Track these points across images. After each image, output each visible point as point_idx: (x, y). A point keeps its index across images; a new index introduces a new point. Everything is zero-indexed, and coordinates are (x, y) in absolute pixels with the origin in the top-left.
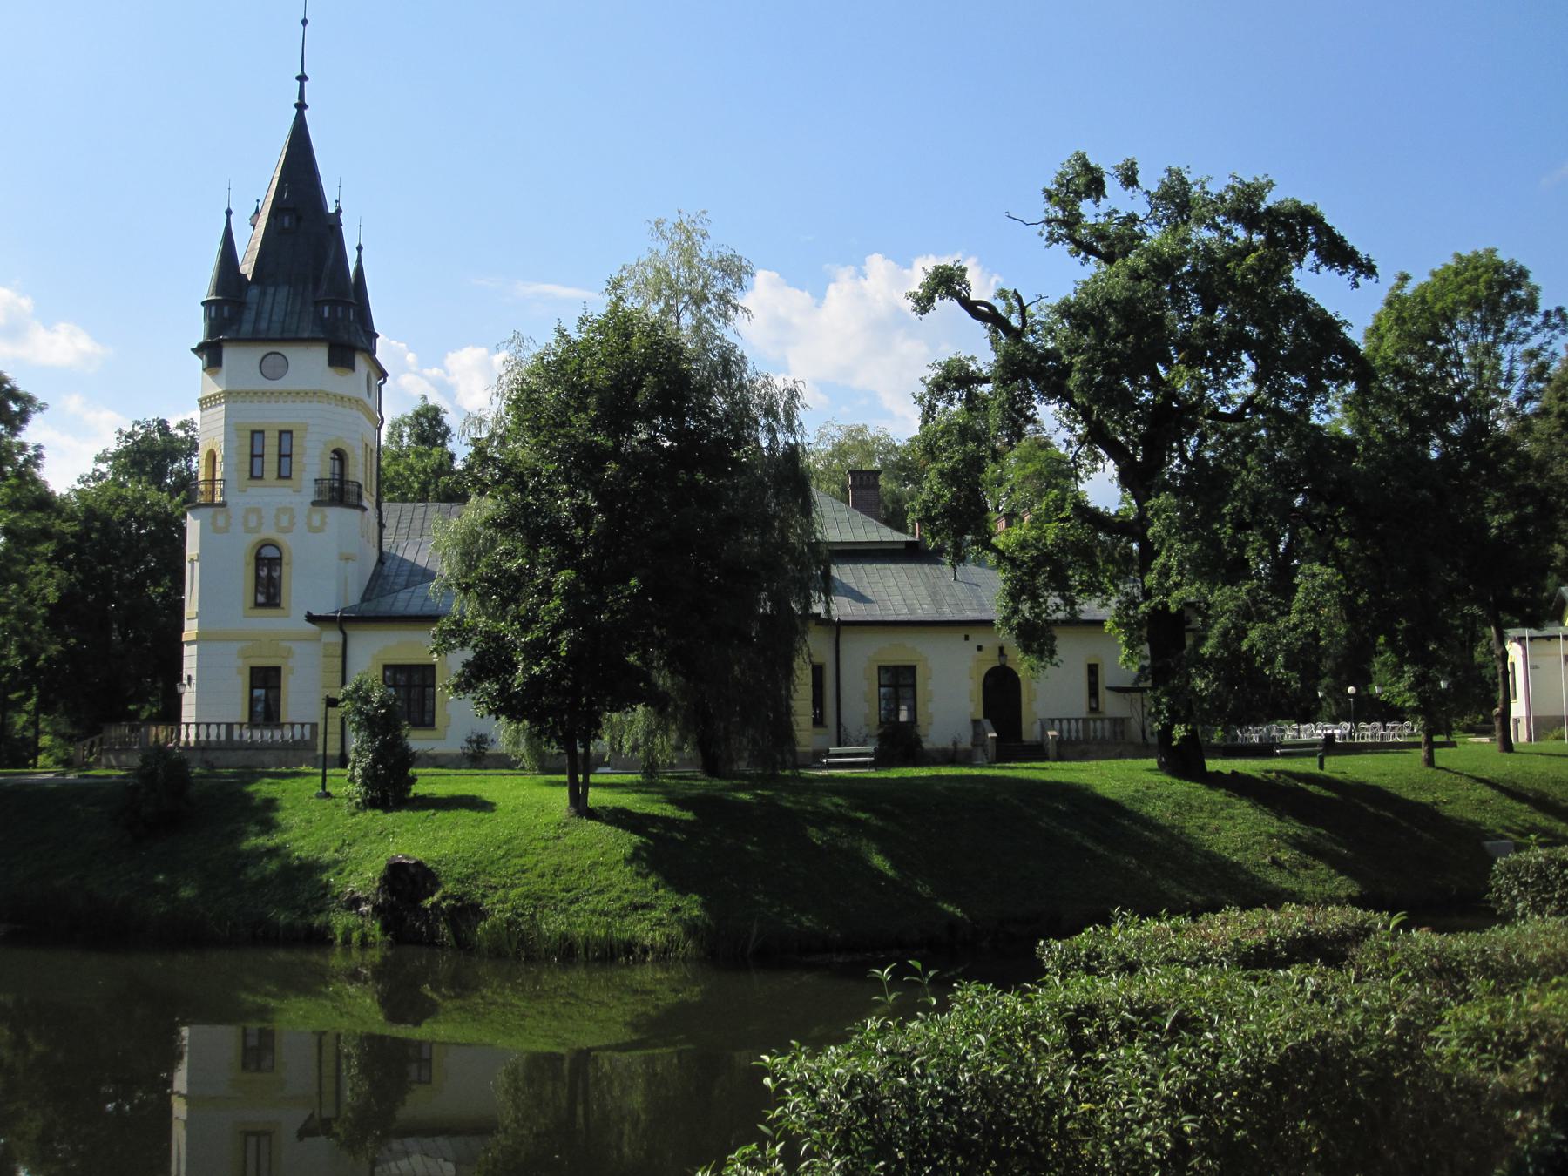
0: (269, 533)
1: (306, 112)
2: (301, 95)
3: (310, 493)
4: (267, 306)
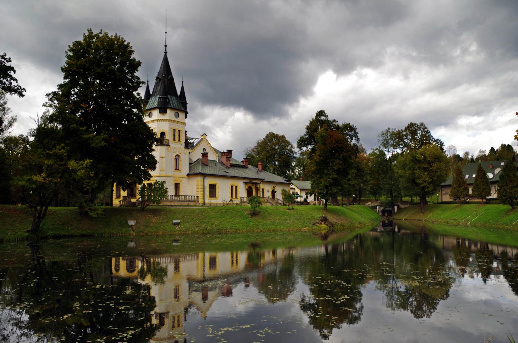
2: (166, 50)
3: (184, 145)
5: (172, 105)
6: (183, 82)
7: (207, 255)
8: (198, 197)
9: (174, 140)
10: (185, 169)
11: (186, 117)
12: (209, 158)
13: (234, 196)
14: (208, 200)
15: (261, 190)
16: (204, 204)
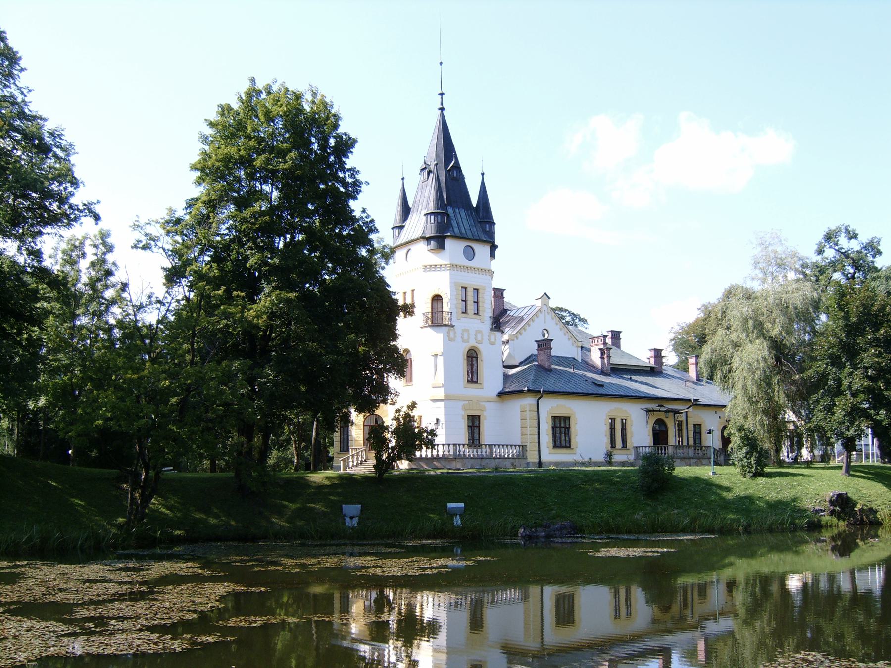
0: (472, 343)
1: (444, 112)
2: (442, 104)
4: (460, 221)
5: (456, 230)
6: (483, 174)
7: (550, 592)
8: (523, 447)
9: (465, 312)
10: (492, 379)
11: (492, 256)
12: (554, 353)
13: (619, 444)
14: (551, 456)
15: (691, 428)
16: (540, 464)
